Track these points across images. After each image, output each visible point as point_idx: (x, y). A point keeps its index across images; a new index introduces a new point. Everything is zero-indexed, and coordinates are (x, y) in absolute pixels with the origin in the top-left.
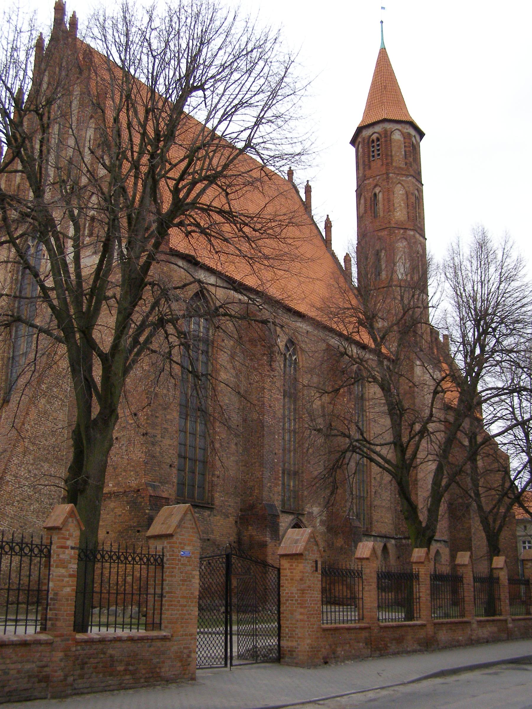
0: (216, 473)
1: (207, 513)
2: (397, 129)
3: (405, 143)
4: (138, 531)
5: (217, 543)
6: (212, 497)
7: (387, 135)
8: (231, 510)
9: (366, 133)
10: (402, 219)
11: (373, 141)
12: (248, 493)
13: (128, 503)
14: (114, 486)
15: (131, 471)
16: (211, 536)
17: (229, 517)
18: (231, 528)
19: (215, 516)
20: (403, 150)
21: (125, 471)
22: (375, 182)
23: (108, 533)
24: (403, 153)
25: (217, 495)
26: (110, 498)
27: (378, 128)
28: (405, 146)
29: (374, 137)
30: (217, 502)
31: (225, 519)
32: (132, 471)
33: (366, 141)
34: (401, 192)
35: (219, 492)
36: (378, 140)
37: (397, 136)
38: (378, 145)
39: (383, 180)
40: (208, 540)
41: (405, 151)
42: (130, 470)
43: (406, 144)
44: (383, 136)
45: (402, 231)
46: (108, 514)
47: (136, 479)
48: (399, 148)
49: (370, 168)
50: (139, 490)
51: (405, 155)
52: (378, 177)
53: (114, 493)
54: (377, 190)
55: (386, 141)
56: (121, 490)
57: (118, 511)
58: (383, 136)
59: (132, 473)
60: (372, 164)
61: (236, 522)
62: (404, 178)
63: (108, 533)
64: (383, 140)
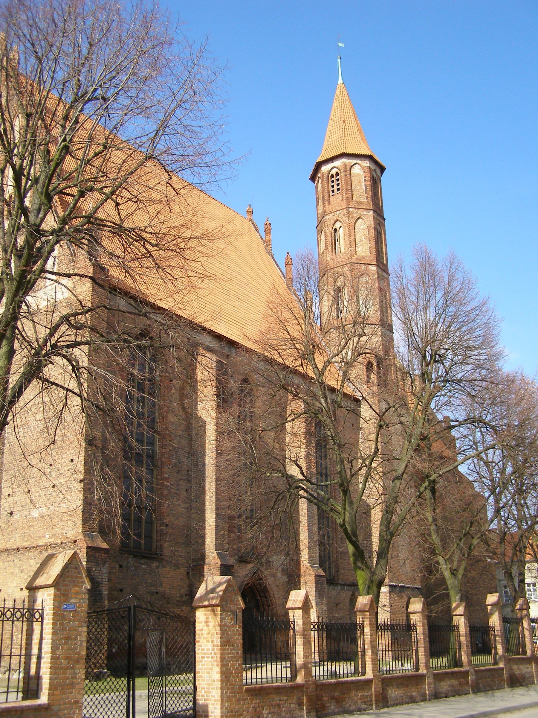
0: (165, 521)
1: (155, 564)
2: (356, 163)
3: (365, 177)
5: (166, 596)
6: (161, 546)
7: (348, 170)
8: (182, 561)
10: (363, 254)
11: (332, 176)
12: (200, 541)
16: (160, 589)
17: (179, 568)
18: (182, 579)
19: (165, 567)
20: (363, 184)
22: (335, 218)
24: (364, 187)
25: (166, 545)
27: (337, 163)
28: (365, 180)
29: (334, 172)
30: (166, 552)
31: (175, 570)
32: (70, 520)
33: (325, 176)
34: (362, 227)
35: (168, 541)
36: (337, 174)
38: (338, 180)
39: (344, 215)
40: (157, 593)
41: (366, 185)
43: (367, 178)
44: (342, 171)
45: (363, 267)
48: (360, 182)
49: (330, 203)
50: (75, 541)
51: (366, 189)
52: (338, 212)
55: (346, 175)
58: (342, 171)
59: (69, 523)
60: (332, 199)
61: (188, 573)
62: (365, 213)
64: (343, 174)
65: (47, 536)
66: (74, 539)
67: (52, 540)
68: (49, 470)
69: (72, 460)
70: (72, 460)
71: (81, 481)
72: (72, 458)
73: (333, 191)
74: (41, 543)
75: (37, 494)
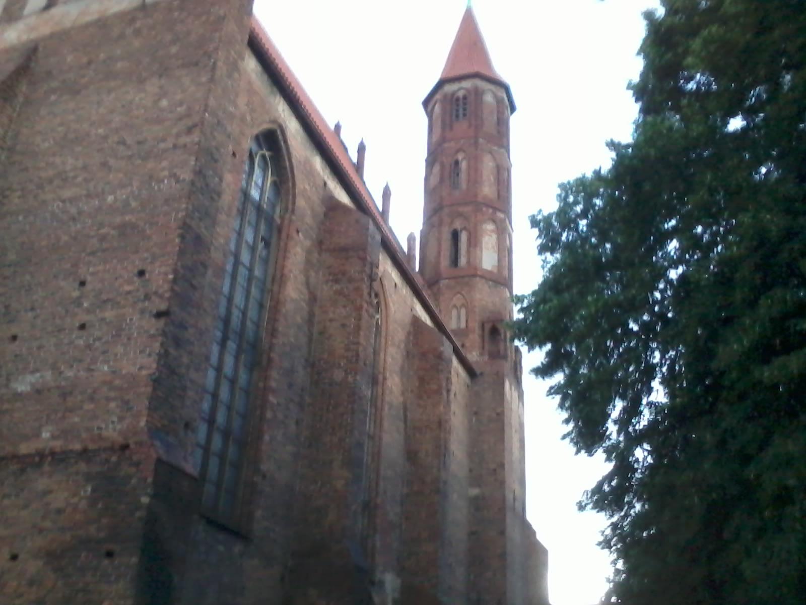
1: (238, 548)
4: (110, 554)
7: (478, 94)
9: (449, 88)
13: (88, 478)
14: (53, 437)
15: (108, 399)
21: (92, 399)
23: (14, 557)
25: (259, 513)
26: (39, 465)
27: (467, 84)
29: (461, 94)
37: (489, 98)
42: (108, 399)
46: (26, 507)
47: (121, 419)
50: (125, 447)
53: (53, 453)
54: (460, 156)
56: (77, 446)
57: (59, 499)
59: (113, 405)
63: (14, 557)
65: (46, 435)
66: (120, 440)
67: (58, 444)
68: (76, 294)
69: (141, 273)
70: (141, 273)
71: (159, 315)
72: (140, 267)
73: (457, 116)
74: (24, 448)
75: (35, 344)
